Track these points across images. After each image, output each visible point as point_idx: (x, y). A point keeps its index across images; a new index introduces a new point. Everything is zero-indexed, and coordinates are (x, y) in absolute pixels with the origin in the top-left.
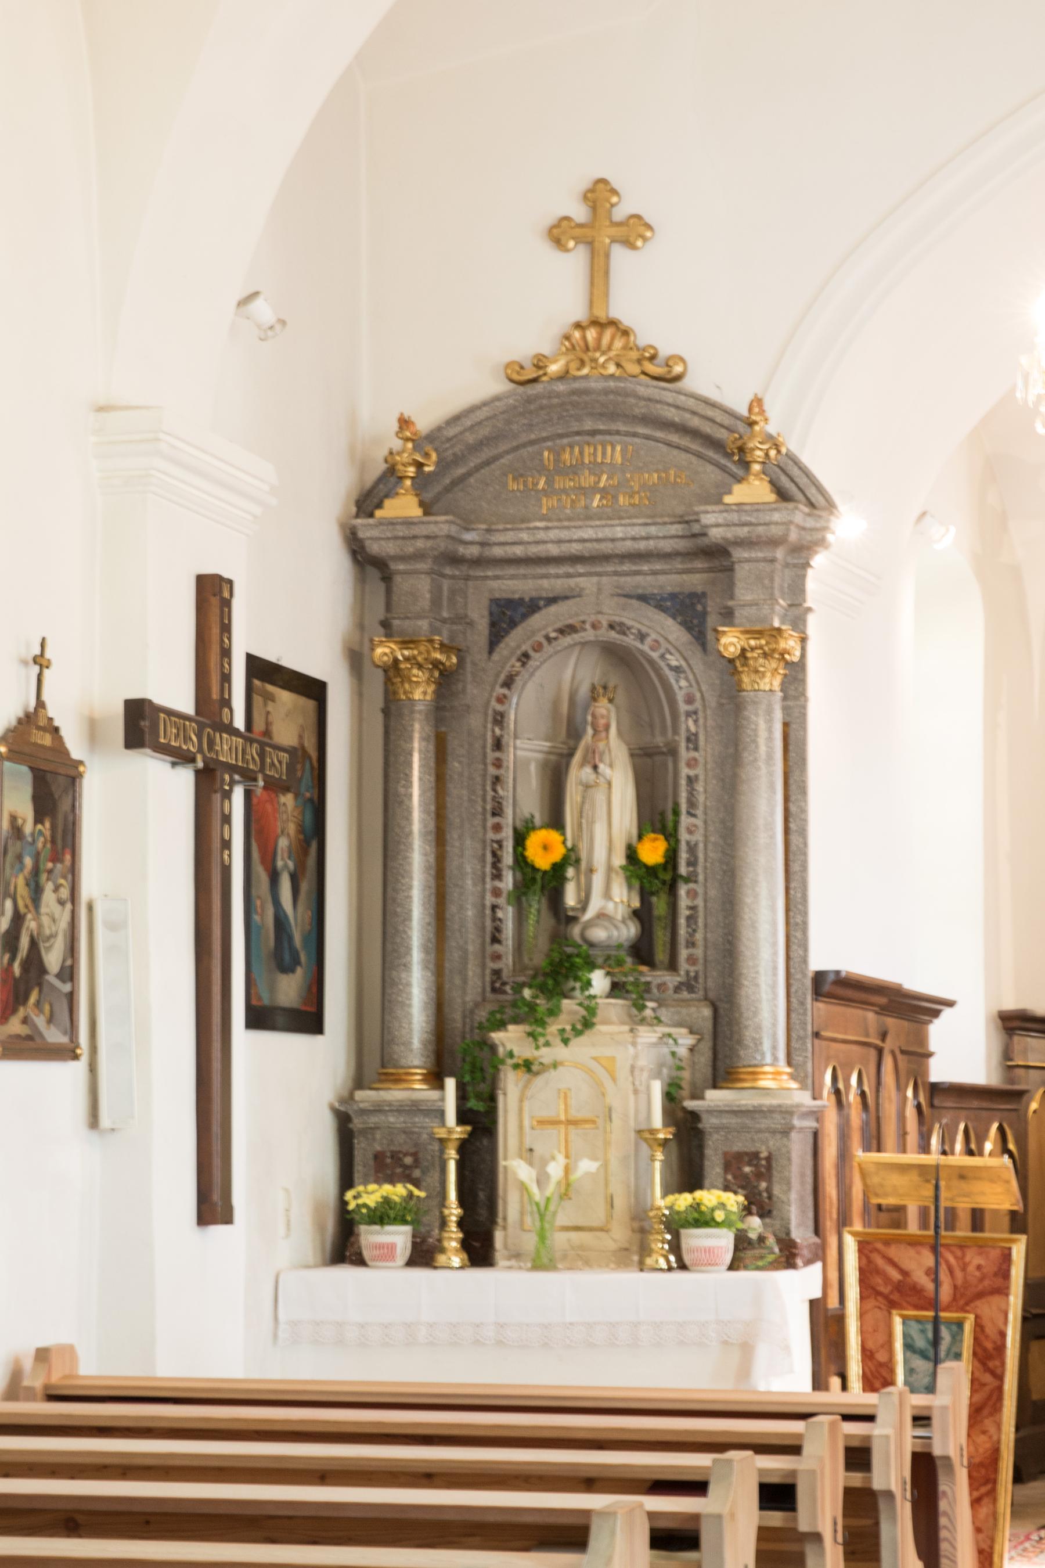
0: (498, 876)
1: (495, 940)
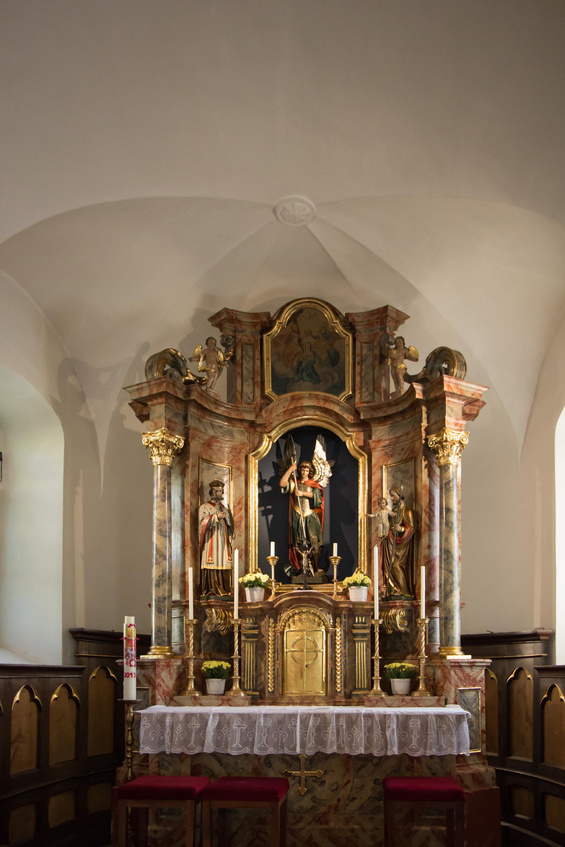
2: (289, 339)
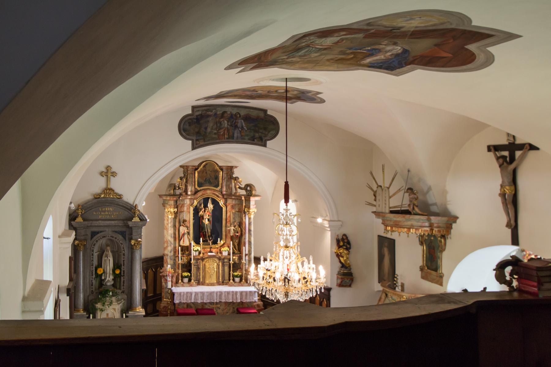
2: (203, 172)
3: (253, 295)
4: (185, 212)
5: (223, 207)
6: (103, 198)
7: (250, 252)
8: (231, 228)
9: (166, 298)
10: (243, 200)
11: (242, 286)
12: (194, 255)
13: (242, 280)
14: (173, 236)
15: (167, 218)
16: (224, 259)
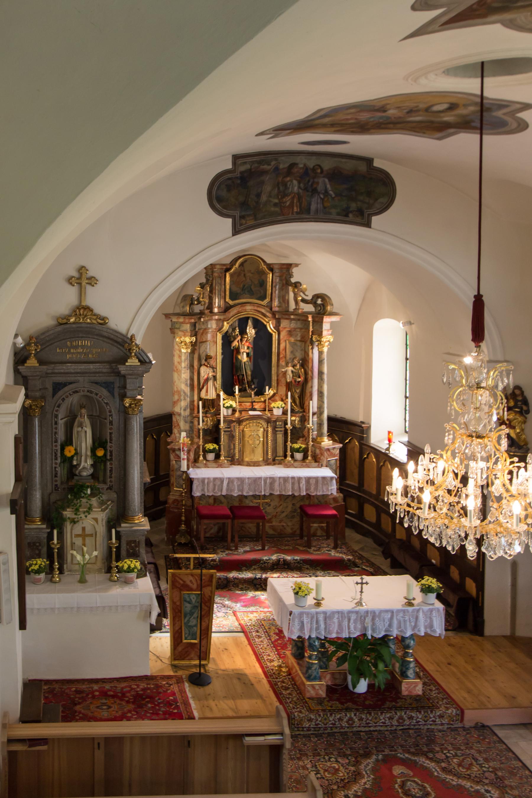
0: (56, 459)
1: (56, 476)
3: (327, 484)
4: (208, 343)
5: (274, 334)
6: (74, 323)
7: (322, 410)
8: (286, 368)
9: (178, 486)
10: (309, 321)
11: (308, 467)
12: (225, 414)
13: (307, 457)
14: (189, 382)
15: (178, 352)
16: (275, 422)
